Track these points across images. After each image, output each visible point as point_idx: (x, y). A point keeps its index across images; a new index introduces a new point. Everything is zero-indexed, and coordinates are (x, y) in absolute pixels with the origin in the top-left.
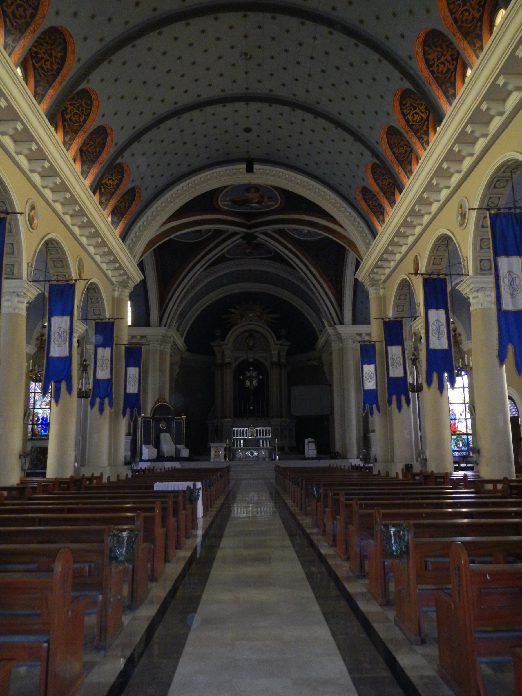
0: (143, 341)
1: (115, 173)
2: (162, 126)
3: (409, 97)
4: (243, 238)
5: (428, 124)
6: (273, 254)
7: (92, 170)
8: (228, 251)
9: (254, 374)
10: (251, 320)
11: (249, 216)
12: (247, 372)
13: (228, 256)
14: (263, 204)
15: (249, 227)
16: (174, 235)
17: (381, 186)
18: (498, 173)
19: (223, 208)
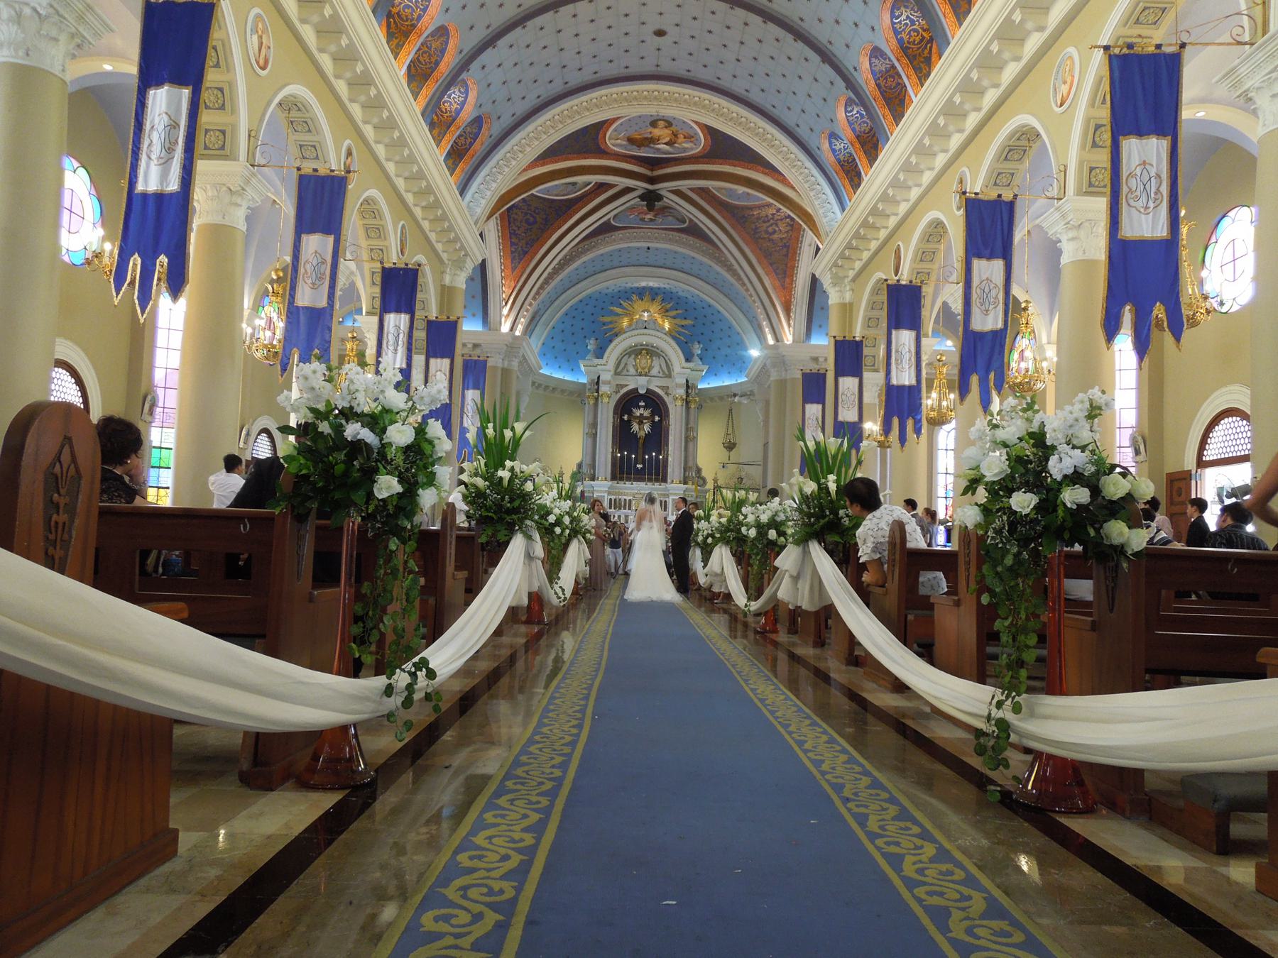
1: (454, 92)
2: (529, 24)
3: (906, 7)
4: (642, 197)
5: (931, 47)
6: (685, 225)
7: (424, 90)
8: (615, 216)
9: (647, 413)
11: (653, 163)
13: (614, 223)
14: (676, 145)
15: (652, 180)
16: (537, 189)
17: (858, 133)
18: (1011, 139)
19: (612, 150)
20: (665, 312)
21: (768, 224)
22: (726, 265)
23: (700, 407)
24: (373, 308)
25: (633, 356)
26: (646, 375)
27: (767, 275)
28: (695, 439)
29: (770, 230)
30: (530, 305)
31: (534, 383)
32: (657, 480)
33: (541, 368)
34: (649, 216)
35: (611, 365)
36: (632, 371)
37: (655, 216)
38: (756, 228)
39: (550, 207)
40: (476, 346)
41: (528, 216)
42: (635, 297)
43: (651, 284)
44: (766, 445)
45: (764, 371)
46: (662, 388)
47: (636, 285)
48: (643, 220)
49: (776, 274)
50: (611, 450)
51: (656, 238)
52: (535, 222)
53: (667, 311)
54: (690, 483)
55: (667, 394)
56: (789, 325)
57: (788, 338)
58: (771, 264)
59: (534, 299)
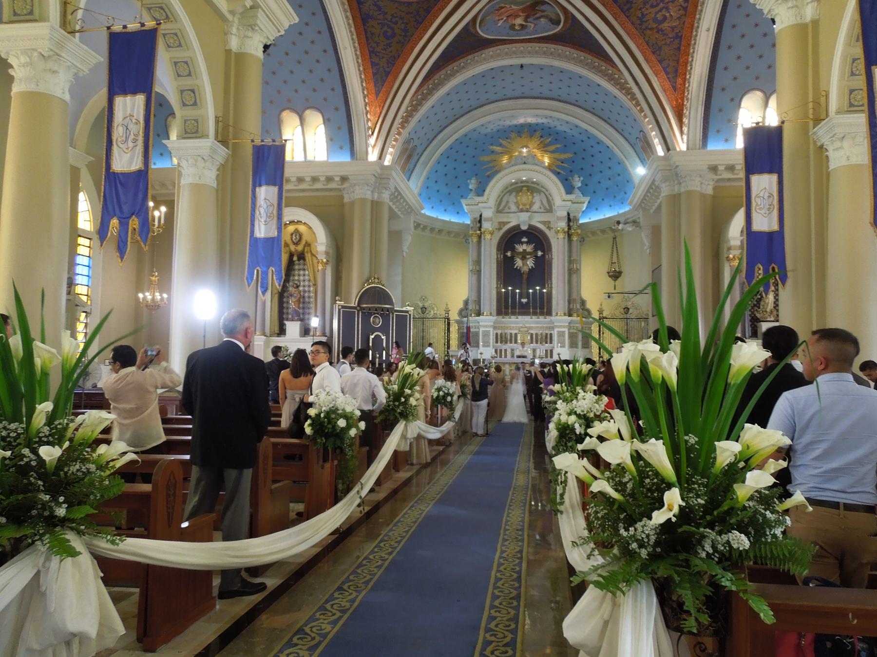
0: (346, 185)
9: (529, 248)
10: (525, 163)
12: (517, 246)
20: (544, 147)
21: (658, 8)
22: (606, 75)
23: (582, 240)
24: (15, 14)
25: (514, 194)
26: (527, 211)
27: (656, 76)
28: (578, 271)
29: (659, 17)
30: (399, 134)
31: (417, 226)
32: (542, 314)
33: (422, 208)
34: (519, 21)
35: (492, 202)
36: (513, 208)
37: (526, 21)
38: (643, 16)
39: (407, 13)
40: (344, 179)
41: (386, 28)
42: (513, 135)
43: (530, 120)
44: (656, 270)
45: (652, 189)
46: (544, 223)
47: (515, 122)
48: (512, 27)
49: (667, 73)
50: (495, 286)
51: (529, 53)
52: (393, 35)
53: (544, 147)
54: (575, 315)
55: (549, 228)
56: (682, 133)
57: (681, 144)
58: (660, 62)
59: (403, 125)
